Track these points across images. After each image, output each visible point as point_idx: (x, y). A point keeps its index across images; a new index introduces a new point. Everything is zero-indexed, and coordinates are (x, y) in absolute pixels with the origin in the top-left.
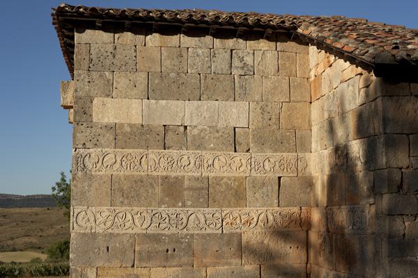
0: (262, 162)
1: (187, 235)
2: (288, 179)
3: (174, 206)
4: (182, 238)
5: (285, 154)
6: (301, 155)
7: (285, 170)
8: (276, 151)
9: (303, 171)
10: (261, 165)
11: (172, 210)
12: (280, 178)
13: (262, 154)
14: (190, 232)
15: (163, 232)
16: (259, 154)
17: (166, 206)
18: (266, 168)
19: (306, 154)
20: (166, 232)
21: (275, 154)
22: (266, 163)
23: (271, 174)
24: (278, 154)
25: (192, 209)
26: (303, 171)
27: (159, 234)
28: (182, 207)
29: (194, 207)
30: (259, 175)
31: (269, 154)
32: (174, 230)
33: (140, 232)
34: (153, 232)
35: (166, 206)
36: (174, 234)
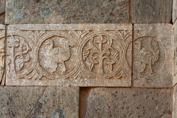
0: (35, 49)
2: (106, 93)
5: (98, 28)
6: (143, 29)
7: (99, 71)
8: (74, 18)
9: (149, 73)
10: (33, 55)
12: (84, 90)
13: (38, 27)
16: (29, 26)
18: (47, 63)
19: (159, 27)
21: (69, 27)
22: (48, 53)
23: (59, 82)
24: (80, 26)
26: (149, 73)
30: (24, 82)
31: (55, 25)
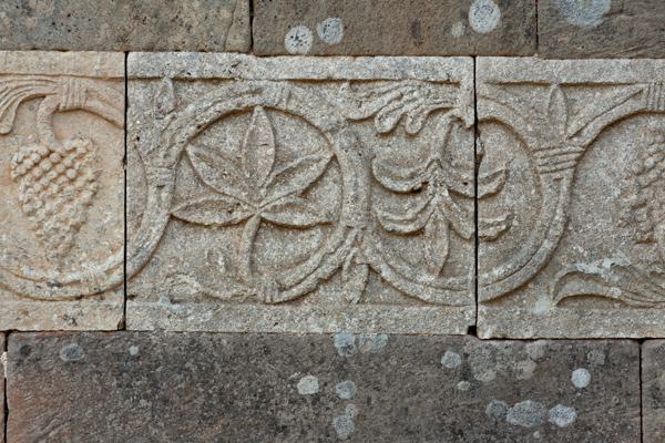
1: (571, 353)
3: (418, 39)
4: (513, 390)
11: (404, 81)
14: (603, 326)
15: (305, 323)
17: (333, 31)
20: (335, 320)
25: (618, 69)
27: (268, 346)
28: (504, 42)
29: (638, 49)
32: (428, 308)
33: (48, 318)
34: (197, 320)
35: (333, 31)
36: (425, 352)
